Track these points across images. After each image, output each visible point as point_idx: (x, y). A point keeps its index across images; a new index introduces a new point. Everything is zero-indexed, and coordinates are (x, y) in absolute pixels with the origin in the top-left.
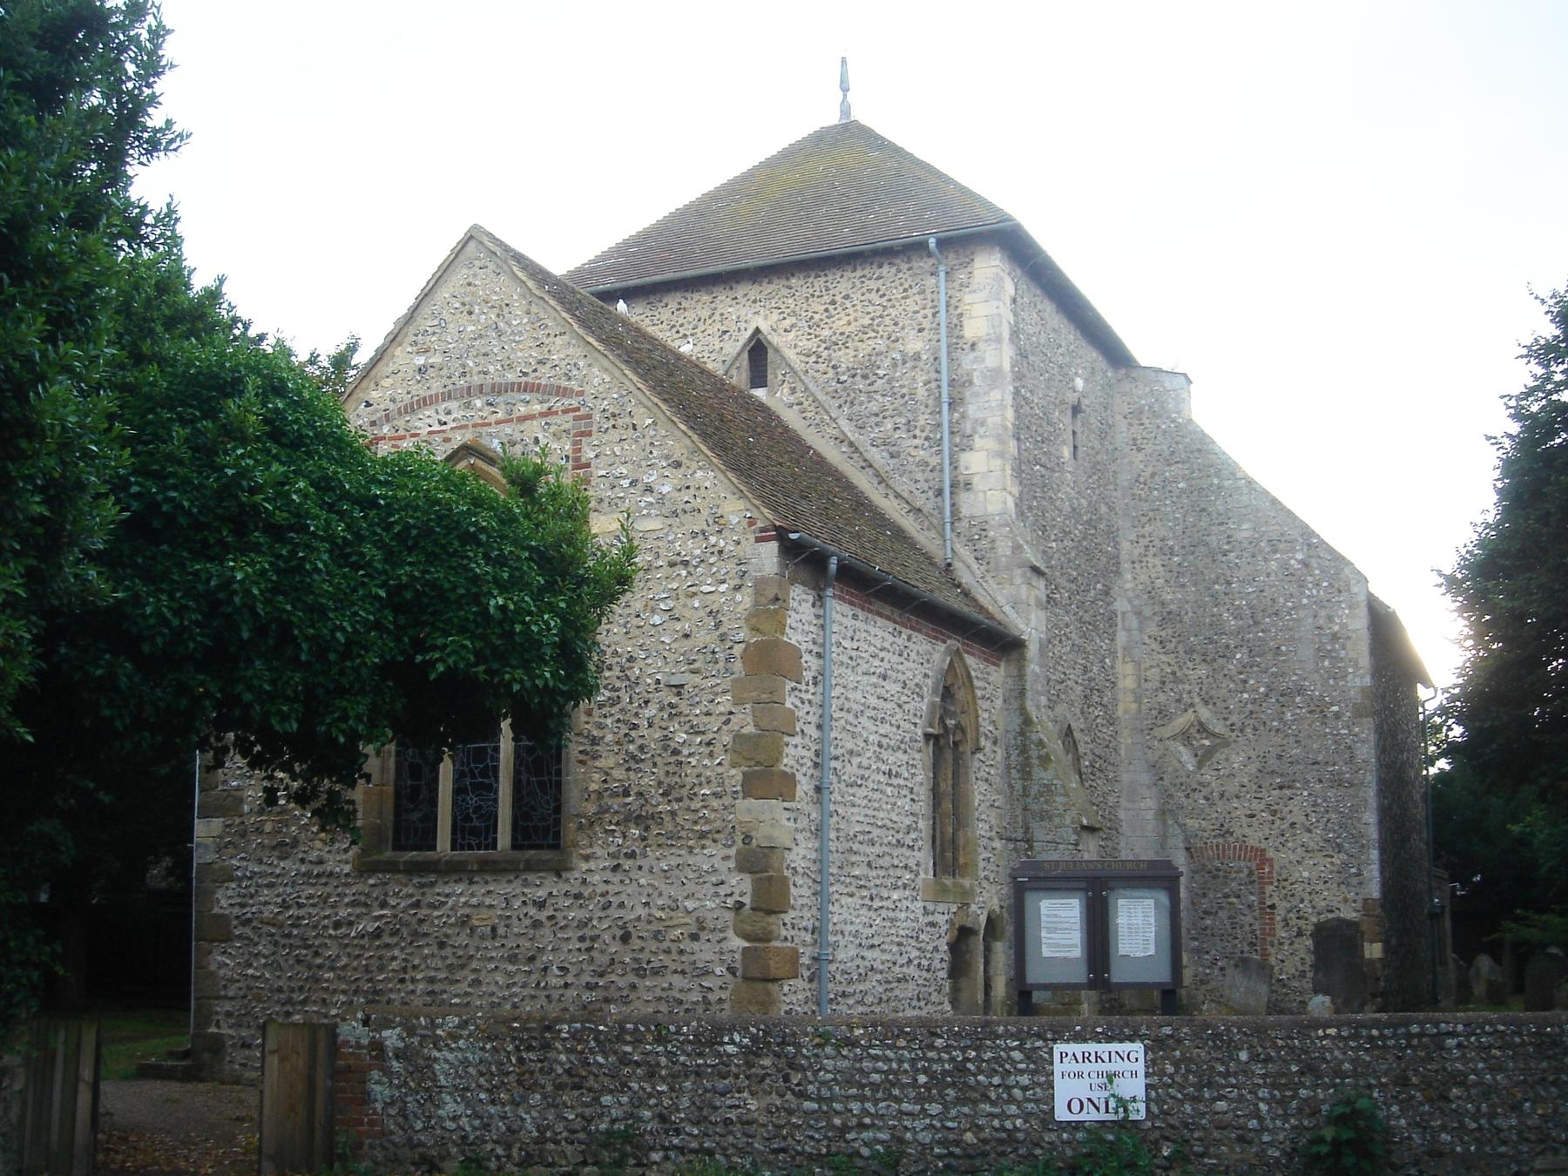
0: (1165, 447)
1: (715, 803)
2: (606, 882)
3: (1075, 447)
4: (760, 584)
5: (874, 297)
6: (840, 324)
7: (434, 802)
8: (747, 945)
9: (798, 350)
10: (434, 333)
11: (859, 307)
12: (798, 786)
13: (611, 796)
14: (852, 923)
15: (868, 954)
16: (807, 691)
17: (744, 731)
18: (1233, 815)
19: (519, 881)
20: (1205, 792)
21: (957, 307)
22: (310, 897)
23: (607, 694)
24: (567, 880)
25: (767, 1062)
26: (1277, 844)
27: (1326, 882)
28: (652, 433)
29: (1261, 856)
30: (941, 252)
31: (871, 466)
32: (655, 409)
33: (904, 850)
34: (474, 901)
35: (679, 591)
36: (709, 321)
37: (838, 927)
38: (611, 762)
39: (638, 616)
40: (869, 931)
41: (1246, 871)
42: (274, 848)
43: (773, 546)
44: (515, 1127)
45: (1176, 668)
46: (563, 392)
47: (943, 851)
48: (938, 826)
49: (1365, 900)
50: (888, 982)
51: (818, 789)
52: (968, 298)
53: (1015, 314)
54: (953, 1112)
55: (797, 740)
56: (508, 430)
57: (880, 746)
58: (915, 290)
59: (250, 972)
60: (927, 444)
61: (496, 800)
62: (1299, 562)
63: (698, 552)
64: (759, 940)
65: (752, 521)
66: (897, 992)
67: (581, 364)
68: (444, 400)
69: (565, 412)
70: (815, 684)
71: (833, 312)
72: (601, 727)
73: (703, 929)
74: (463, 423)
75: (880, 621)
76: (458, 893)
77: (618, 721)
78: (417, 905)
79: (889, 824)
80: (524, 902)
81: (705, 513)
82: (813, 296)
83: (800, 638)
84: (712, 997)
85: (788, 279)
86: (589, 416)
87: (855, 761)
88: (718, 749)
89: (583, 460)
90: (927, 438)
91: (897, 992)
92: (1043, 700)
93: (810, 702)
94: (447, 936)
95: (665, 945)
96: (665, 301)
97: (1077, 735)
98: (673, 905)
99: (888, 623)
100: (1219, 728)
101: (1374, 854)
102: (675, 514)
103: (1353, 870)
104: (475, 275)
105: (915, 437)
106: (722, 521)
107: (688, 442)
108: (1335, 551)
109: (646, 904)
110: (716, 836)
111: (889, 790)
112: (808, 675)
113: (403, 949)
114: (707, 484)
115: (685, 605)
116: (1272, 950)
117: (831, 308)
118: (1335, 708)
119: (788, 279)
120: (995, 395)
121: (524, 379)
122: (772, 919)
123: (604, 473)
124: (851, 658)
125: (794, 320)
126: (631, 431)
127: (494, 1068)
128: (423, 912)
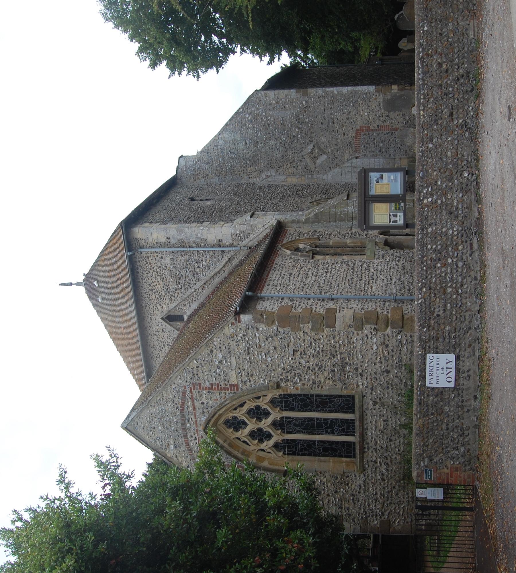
0: (207, 166)
1: (337, 338)
2: (367, 379)
3: (206, 200)
4: (257, 321)
5: (150, 275)
6: (159, 287)
7: (337, 443)
8: (389, 327)
9: (169, 303)
10: (162, 442)
11: (154, 281)
12: (331, 307)
13: (335, 377)
14: (382, 287)
15: (394, 280)
16: (296, 304)
17: (310, 327)
19: (367, 412)
20: (335, 152)
21: (154, 244)
22: (373, 489)
23: (297, 378)
24: (366, 393)
25: (432, 322)
28: (200, 361)
29: (358, 132)
30: (133, 250)
31: (213, 277)
32: (191, 360)
33: (355, 267)
34: (374, 428)
35: (259, 351)
36: (159, 337)
38: (321, 376)
39: (268, 366)
40: (385, 280)
41: (365, 136)
42: (355, 504)
43: (243, 317)
44: (457, 417)
45: (289, 162)
46: (184, 393)
47: (356, 252)
48: (346, 253)
49: (376, 91)
50: (404, 273)
51: (332, 299)
52: (150, 240)
53: (157, 222)
54: (451, 254)
55: (314, 307)
56: (198, 414)
57: (316, 276)
58: (147, 260)
59: (401, 513)
60: (205, 256)
61: (336, 419)
62: (249, 116)
63: (244, 344)
64: (388, 322)
65: (233, 324)
66: (408, 270)
67: (173, 387)
68: (187, 438)
69: (191, 393)
70: (293, 300)
71: (155, 290)
72: (309, 380)
73: (384, 343)
74: (195, 431)
75: (270, 276)
76: (371, 433)
77: (306, 374)
78: (376, 450)
79: (346, 272)
80: (374, 409)
81: (229, 341)
82: (149, 298)
83: (276, 306)
84: (410, 340)
85: (143, 307)
86: (193, 383)
87: (322, 285)
88: (317, 337)
89: (209, 386)
90: (203, 256)
91: (408, 270)
92: (300, 213)
93: (300, 303)
94: (387, 439)
95: (390, 358)
96: (151, 353)
97: (313, 200)
98: (375, 354)
99: (271, 272)
100: (311, 147)
101: (359, 88)
102: (230, 352)
103: (365, 96)
104: (140, 426)
105: (202, 260)
106: (233, 335)
107: (203, 348)
108: (245, 103)
109: (375, 364)
110: (349, 338)
111: (333, 272)
112: (290, 303)
113: (392, 455)
114: (219, 340)
115: (264, 349)
117: (154, 291)
118: (304, 102)
119: (143, 307)
120: (186, 230)
121: (180, 408)
122: (380, 317)
123: (214, 379)
124: (284, 287)
125: (158, 305)
126: (199, 368)
127: (435, 424)
128: (379, 448)
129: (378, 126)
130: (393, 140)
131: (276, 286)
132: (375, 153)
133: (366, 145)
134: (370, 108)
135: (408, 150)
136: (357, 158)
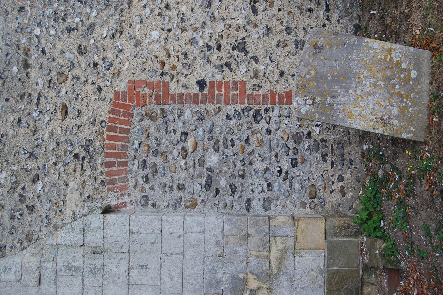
18: (62, 139)
20: (26, 182)
26: (108, 74)
27: (167, 7)
41: (147, 122)
116: (266, 89)
129: (201, 84)
130: (260, 143)
132: (185, 195)
133: (151, 160)
134: (173, 14)
135: (319, 184)
136: (107, 210)
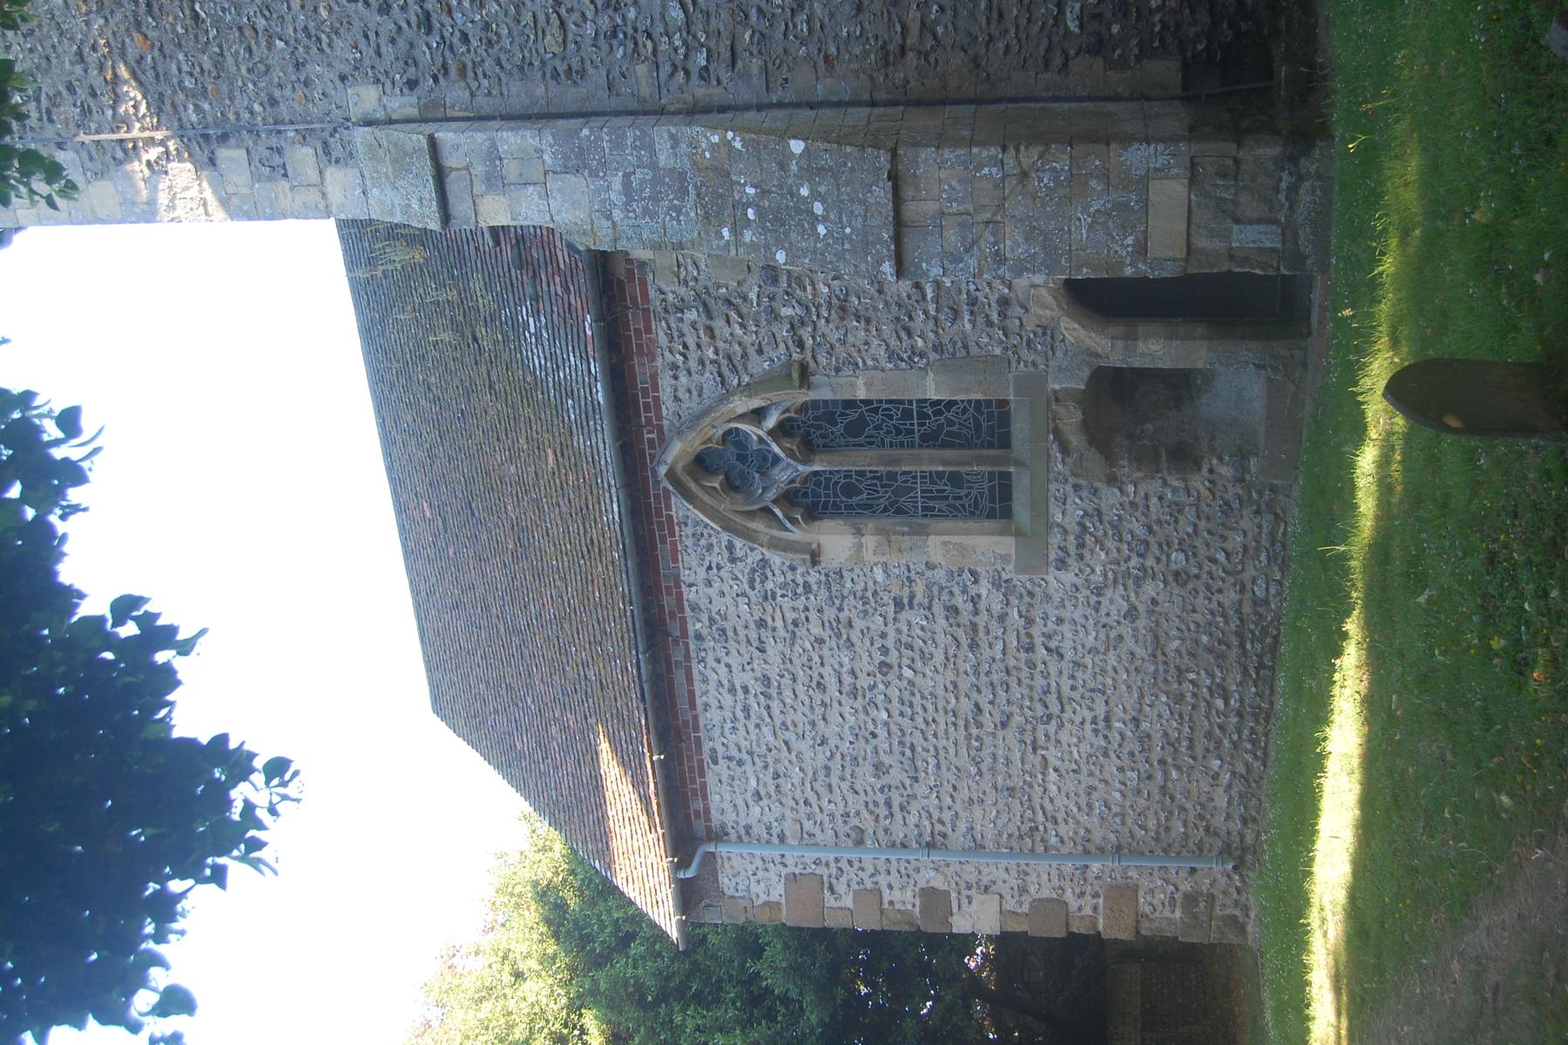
12: (933, 884)
37: (1083, 801)
55: (882, 880)
87: (886, 759)
131: (740, 763)
